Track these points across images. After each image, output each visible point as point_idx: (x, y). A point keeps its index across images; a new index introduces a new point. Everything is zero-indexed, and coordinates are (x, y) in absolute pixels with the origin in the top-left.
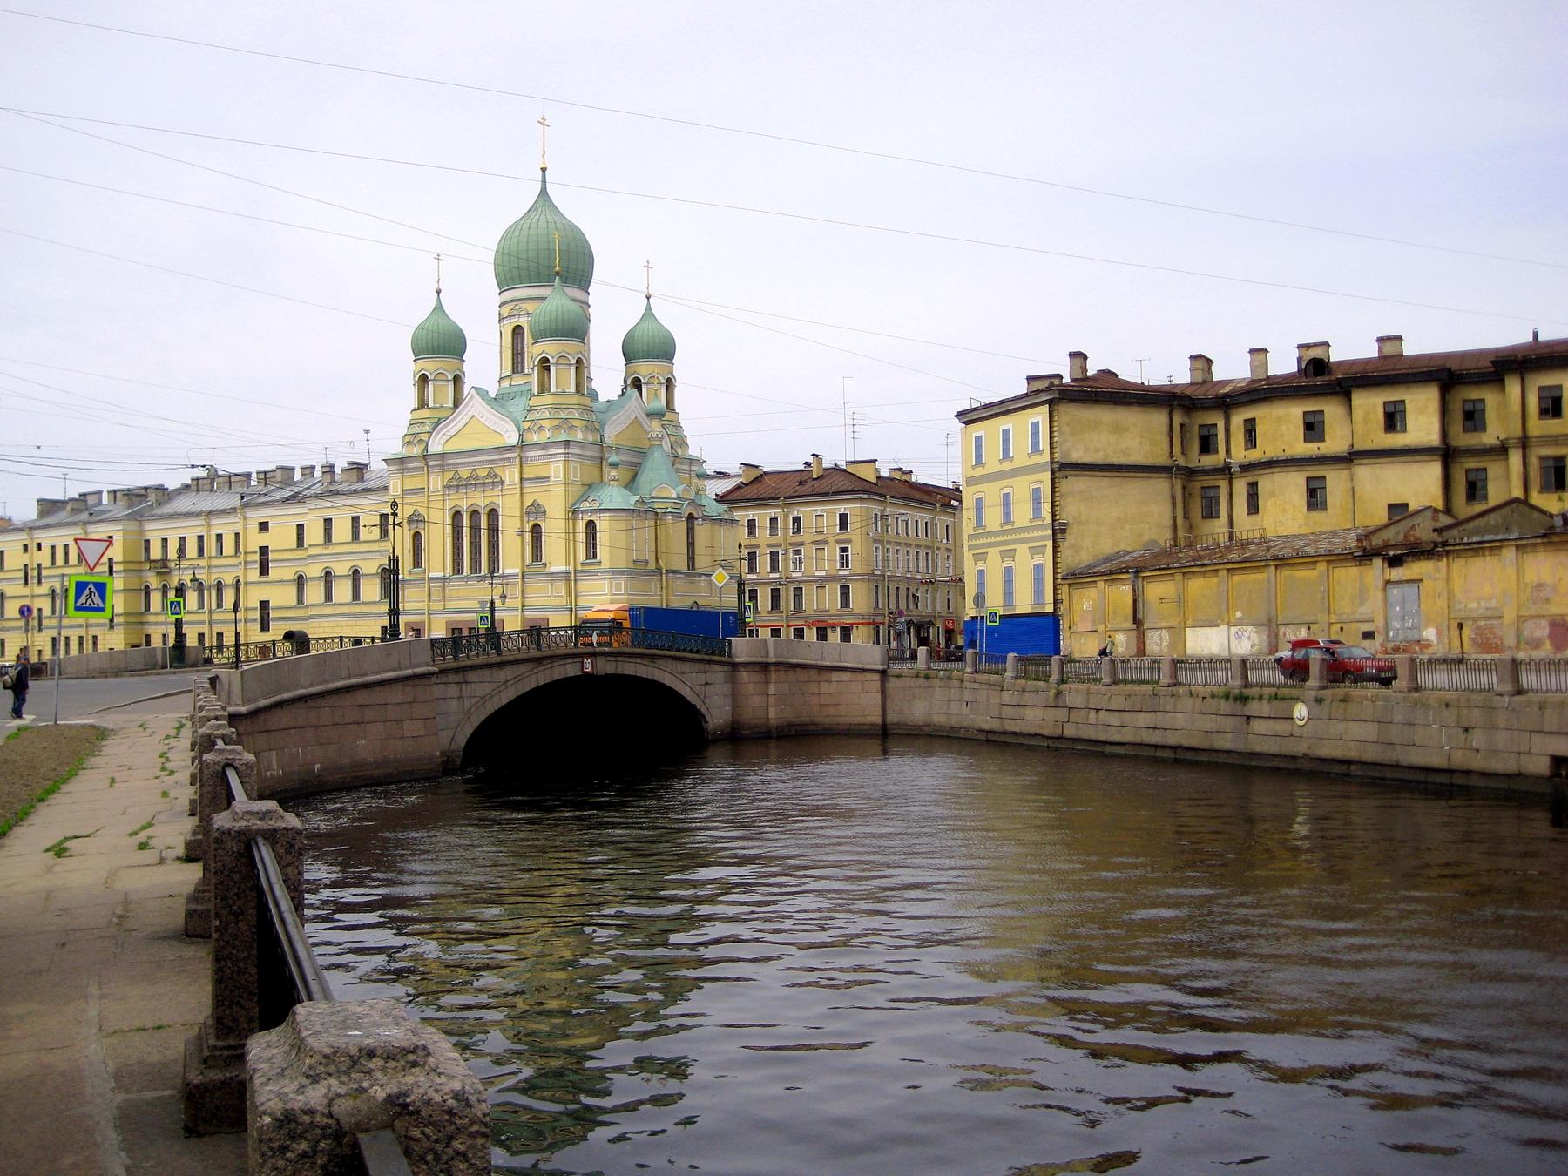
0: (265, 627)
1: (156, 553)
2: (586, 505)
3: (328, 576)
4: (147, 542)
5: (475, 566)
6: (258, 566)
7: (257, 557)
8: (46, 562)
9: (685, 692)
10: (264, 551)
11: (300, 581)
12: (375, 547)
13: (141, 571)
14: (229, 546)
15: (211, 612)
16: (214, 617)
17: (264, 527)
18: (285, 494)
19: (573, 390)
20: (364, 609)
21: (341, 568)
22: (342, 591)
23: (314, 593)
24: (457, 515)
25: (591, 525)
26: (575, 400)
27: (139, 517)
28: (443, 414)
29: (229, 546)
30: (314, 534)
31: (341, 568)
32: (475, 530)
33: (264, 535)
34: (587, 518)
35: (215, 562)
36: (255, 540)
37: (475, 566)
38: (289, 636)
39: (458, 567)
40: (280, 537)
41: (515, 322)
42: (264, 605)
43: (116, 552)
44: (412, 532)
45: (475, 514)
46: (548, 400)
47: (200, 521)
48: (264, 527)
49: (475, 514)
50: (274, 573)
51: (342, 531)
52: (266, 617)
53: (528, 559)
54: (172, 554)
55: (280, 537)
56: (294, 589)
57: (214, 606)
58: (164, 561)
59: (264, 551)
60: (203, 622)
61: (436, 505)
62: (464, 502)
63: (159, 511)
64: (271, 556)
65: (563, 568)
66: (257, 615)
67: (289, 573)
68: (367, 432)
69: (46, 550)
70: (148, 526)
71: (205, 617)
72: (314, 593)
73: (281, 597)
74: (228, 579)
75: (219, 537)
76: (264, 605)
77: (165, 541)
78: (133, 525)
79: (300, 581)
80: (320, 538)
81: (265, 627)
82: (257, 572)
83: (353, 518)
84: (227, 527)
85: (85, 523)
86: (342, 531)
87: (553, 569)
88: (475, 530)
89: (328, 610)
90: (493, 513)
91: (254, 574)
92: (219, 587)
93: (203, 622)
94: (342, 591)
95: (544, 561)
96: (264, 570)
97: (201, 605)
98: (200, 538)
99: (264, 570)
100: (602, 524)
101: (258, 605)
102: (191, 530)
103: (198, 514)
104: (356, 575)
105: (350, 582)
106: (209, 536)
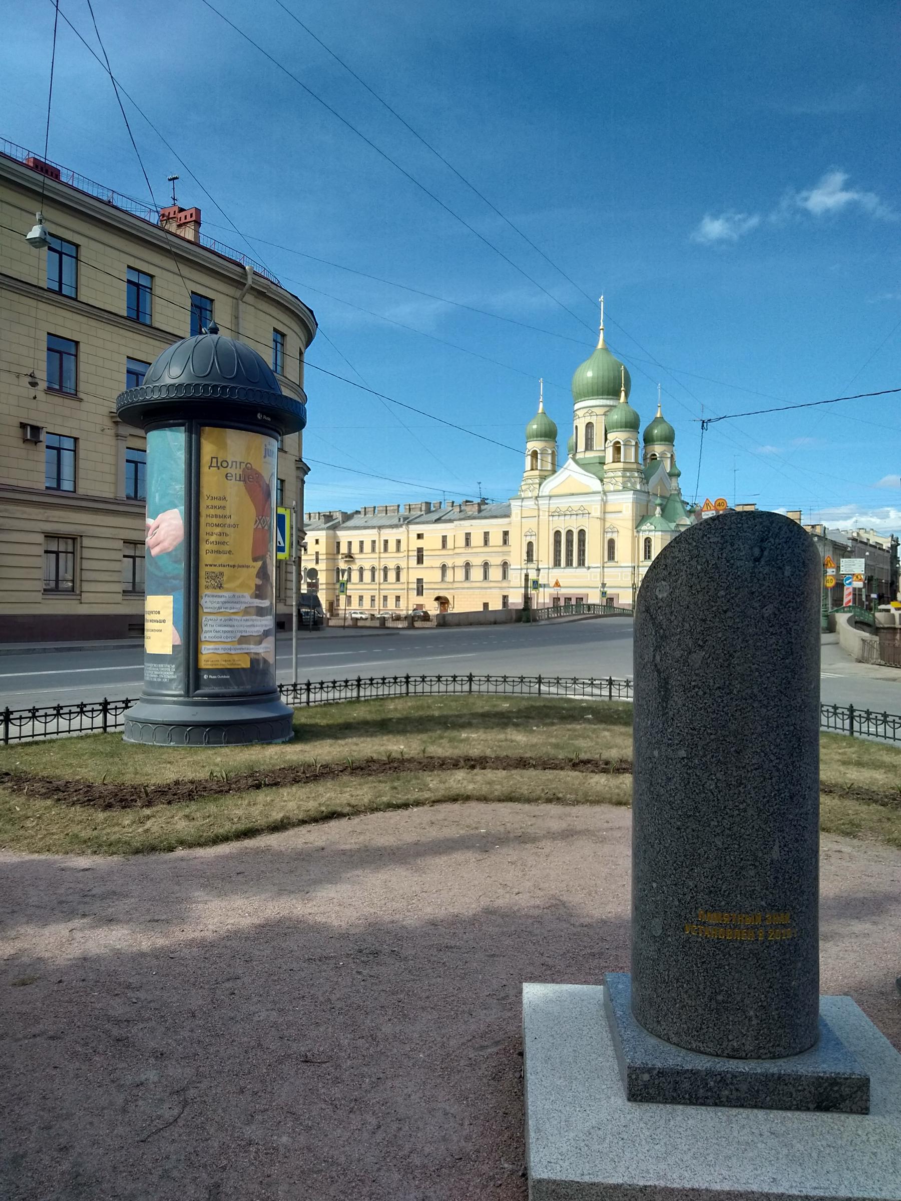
1: (344, 549)
2: (644, 527)
3: (468, 566)
4: (338, 543)
5: (569, 563)
6: (416, 558)
7: (416, 553)
10: (420, 550)
11: (444, 568)
12: (500, 549)
13: (335, 559)
14: (392, 546)
15: (380, 584)
16: (382, 587)
17: (420, 536)
19: (633, 461)
20: (492, 584)
21: (477, 561)
22: (477, 574)
24: (557, 534)
25: (648, 541)
26: (634, 466)
27: (334, 528)
28: (546, 473)
29: (392, 546)
31: (477, 561)
32: (569, 542)
33: (420, 541)
34: (646, 535)
35: (382, 555)
36: (416, 544)
37: (569, 563)
41: (588, 420)
42: (420, 581)
44: (528, 542)
45: (570, 533)
46: (620, 465)
47: (375, 531)
49: (570, 533)
52: (420, 589)
53: (606, 559)
54: (355, 549)
55: (431, 542)
56: (440, 572)
57: (382, 580)
59: (420, 550)
60: (376, 589)
62: (563, 525)
63: (345, 525)
64: (425, 553)
65: (630, 565)
66: (415, 586)
67: (438, 564)
68: (480, 483)
70: (339, 533)
71: (377, 587)
73: (431, 576)
74: (392, 565)
75: (386, 542)
77: (362, 543)
78: (331, 532)
80: (463, 543)
82: (416, 562)
83: (485, 533)
87: (622, 565)
88: (569, 542)
89: (466, 585)
90: (582, 533)
91: (413, 561)
92: (386, 570)
93: (376, 589)
94: (477, 574)
95: (616, 560)
96: (420, 560)
97: (373, 579)
98: (374, 542)
99: (420, 560)
101: (416, 581)
102: (368, 536)
103: (373, 527)
105: (482, 570)
106: (380, 541)
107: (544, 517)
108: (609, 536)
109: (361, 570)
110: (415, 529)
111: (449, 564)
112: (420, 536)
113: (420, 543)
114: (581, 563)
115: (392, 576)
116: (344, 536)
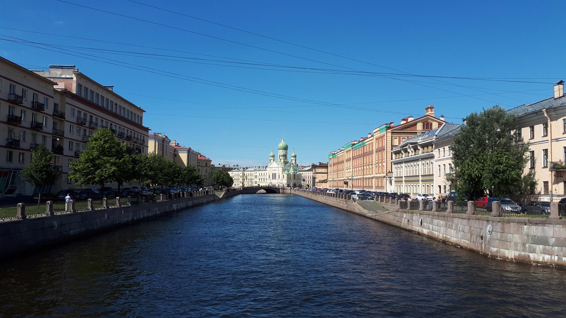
0: (256, 184)
1: (246, 175)
2: (283, 173)
5: (274, 179)
8: (234, 175)
9: (275, 190)
10: (256, 176)
11: (259, 179)
18: (258, 169)
21: (263, 178)
22: (263, 180)
23: (260, 180)
24: (273, 174)
30: (261, 174)
31: (263, 178)
36: (255, 174)
37: (274, 179)
38: (258, 185)
39: (273, 179)
40: (258, 174)
42: (256, 181)
43: (241, 175)
45: (274, 174)
48: (256, 173)
49: (274, 174)
50: (257, 178)
51: (263, 174)
54: (247, 175)
55: (258, 174)
58: (246, 176)
61: (271, 173)
66: (255, 182)
69: (234, 174)
72: (260, 180)
73: (258, 180)
76: (256, 181)
79: (259, 179)
81: (256, 184)
84: (253, 173)
85: (238, 171)
86: (263, 174)
90: (276, 174)
91: (255, 178)
94: (263, 180)
96: (256, 178)
99: (256, 178)
100: (285, 175)
102: (249, 173)
103: (250, 171)
104: (264, 179)
107: (271, 171)
108: (279, 174)
109: (248, 179)
110: (255, 172)
111: (260, 178)
112: (256, 173)
113: (256, 174)
114: (276, 179)
115: (253, 180)
116: (245, 173)
